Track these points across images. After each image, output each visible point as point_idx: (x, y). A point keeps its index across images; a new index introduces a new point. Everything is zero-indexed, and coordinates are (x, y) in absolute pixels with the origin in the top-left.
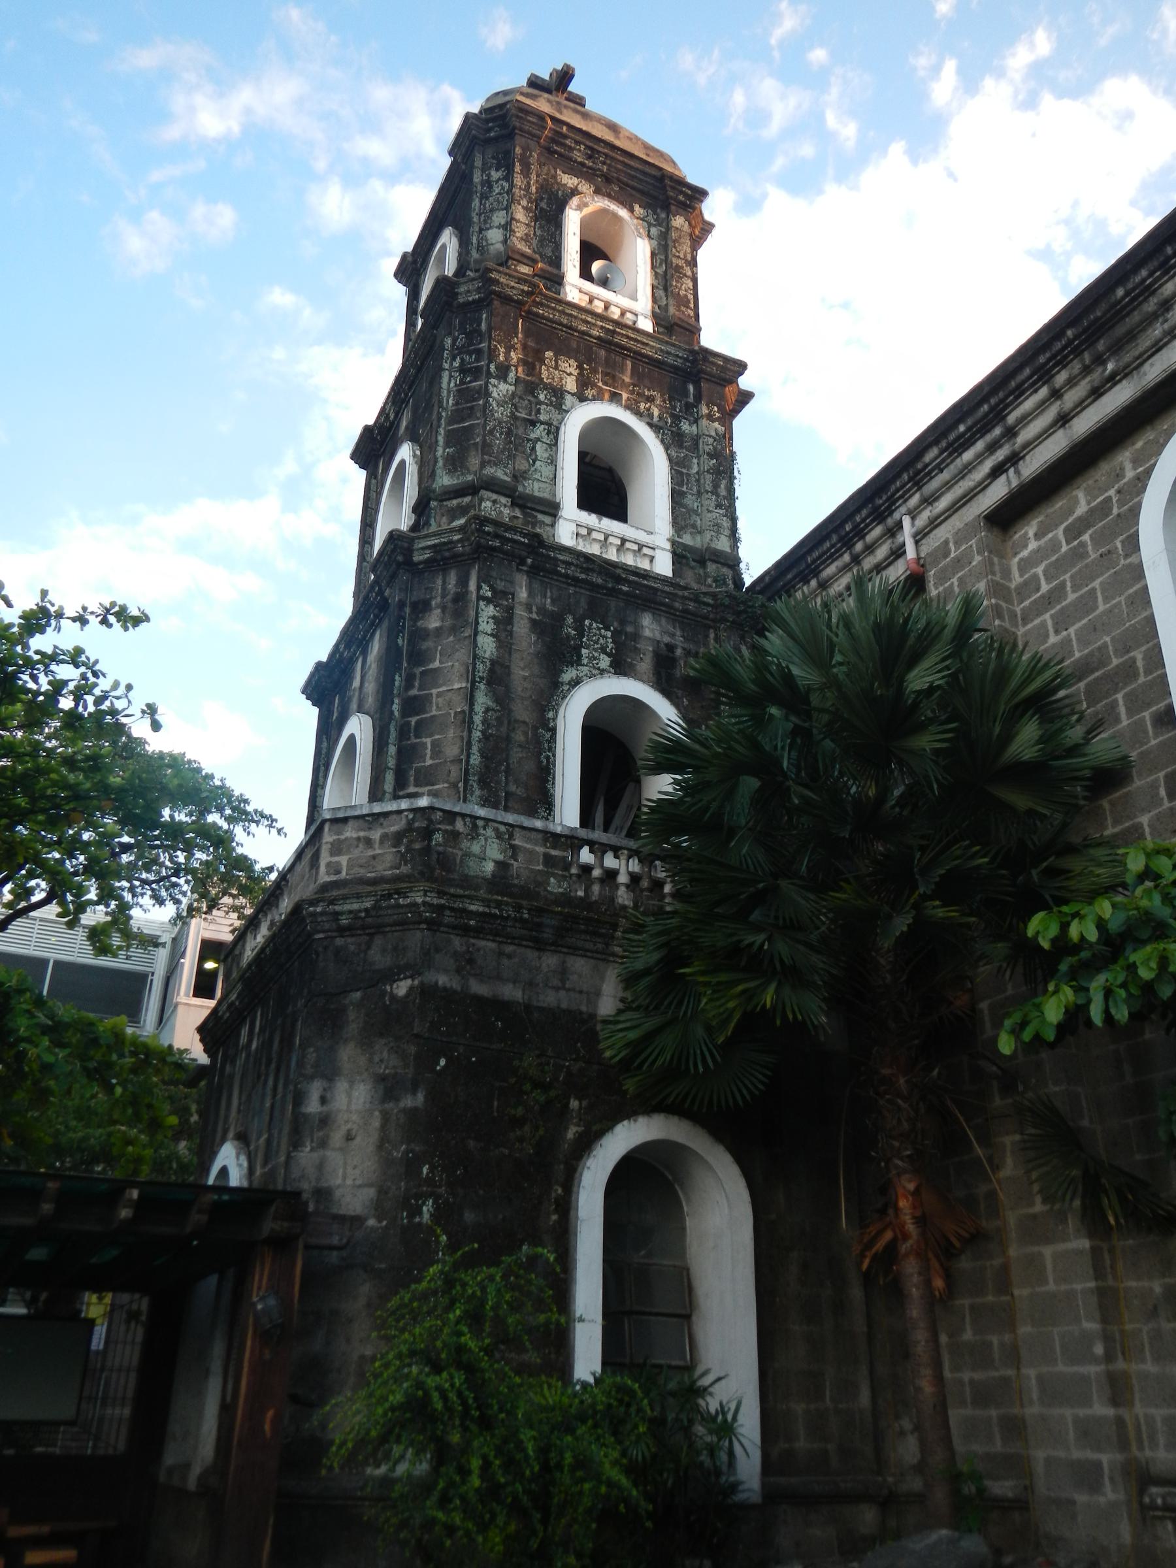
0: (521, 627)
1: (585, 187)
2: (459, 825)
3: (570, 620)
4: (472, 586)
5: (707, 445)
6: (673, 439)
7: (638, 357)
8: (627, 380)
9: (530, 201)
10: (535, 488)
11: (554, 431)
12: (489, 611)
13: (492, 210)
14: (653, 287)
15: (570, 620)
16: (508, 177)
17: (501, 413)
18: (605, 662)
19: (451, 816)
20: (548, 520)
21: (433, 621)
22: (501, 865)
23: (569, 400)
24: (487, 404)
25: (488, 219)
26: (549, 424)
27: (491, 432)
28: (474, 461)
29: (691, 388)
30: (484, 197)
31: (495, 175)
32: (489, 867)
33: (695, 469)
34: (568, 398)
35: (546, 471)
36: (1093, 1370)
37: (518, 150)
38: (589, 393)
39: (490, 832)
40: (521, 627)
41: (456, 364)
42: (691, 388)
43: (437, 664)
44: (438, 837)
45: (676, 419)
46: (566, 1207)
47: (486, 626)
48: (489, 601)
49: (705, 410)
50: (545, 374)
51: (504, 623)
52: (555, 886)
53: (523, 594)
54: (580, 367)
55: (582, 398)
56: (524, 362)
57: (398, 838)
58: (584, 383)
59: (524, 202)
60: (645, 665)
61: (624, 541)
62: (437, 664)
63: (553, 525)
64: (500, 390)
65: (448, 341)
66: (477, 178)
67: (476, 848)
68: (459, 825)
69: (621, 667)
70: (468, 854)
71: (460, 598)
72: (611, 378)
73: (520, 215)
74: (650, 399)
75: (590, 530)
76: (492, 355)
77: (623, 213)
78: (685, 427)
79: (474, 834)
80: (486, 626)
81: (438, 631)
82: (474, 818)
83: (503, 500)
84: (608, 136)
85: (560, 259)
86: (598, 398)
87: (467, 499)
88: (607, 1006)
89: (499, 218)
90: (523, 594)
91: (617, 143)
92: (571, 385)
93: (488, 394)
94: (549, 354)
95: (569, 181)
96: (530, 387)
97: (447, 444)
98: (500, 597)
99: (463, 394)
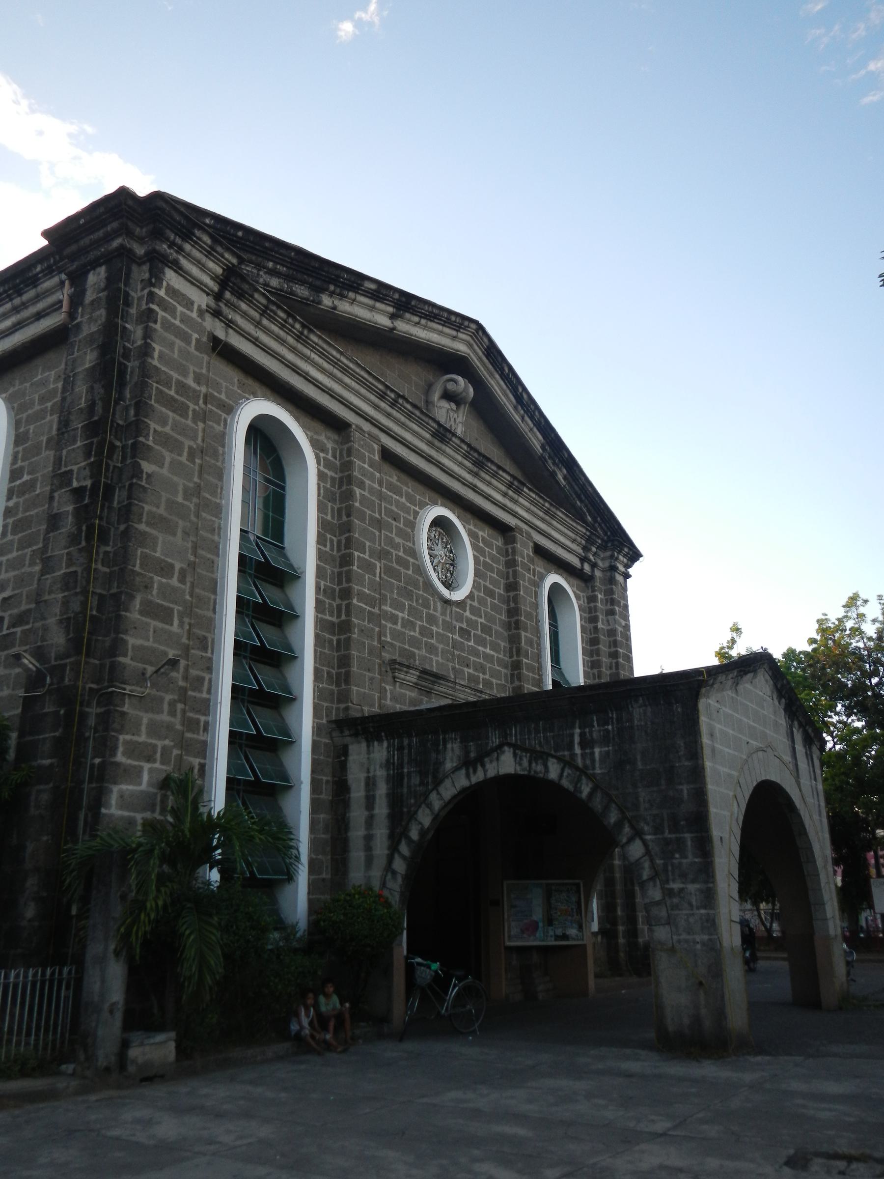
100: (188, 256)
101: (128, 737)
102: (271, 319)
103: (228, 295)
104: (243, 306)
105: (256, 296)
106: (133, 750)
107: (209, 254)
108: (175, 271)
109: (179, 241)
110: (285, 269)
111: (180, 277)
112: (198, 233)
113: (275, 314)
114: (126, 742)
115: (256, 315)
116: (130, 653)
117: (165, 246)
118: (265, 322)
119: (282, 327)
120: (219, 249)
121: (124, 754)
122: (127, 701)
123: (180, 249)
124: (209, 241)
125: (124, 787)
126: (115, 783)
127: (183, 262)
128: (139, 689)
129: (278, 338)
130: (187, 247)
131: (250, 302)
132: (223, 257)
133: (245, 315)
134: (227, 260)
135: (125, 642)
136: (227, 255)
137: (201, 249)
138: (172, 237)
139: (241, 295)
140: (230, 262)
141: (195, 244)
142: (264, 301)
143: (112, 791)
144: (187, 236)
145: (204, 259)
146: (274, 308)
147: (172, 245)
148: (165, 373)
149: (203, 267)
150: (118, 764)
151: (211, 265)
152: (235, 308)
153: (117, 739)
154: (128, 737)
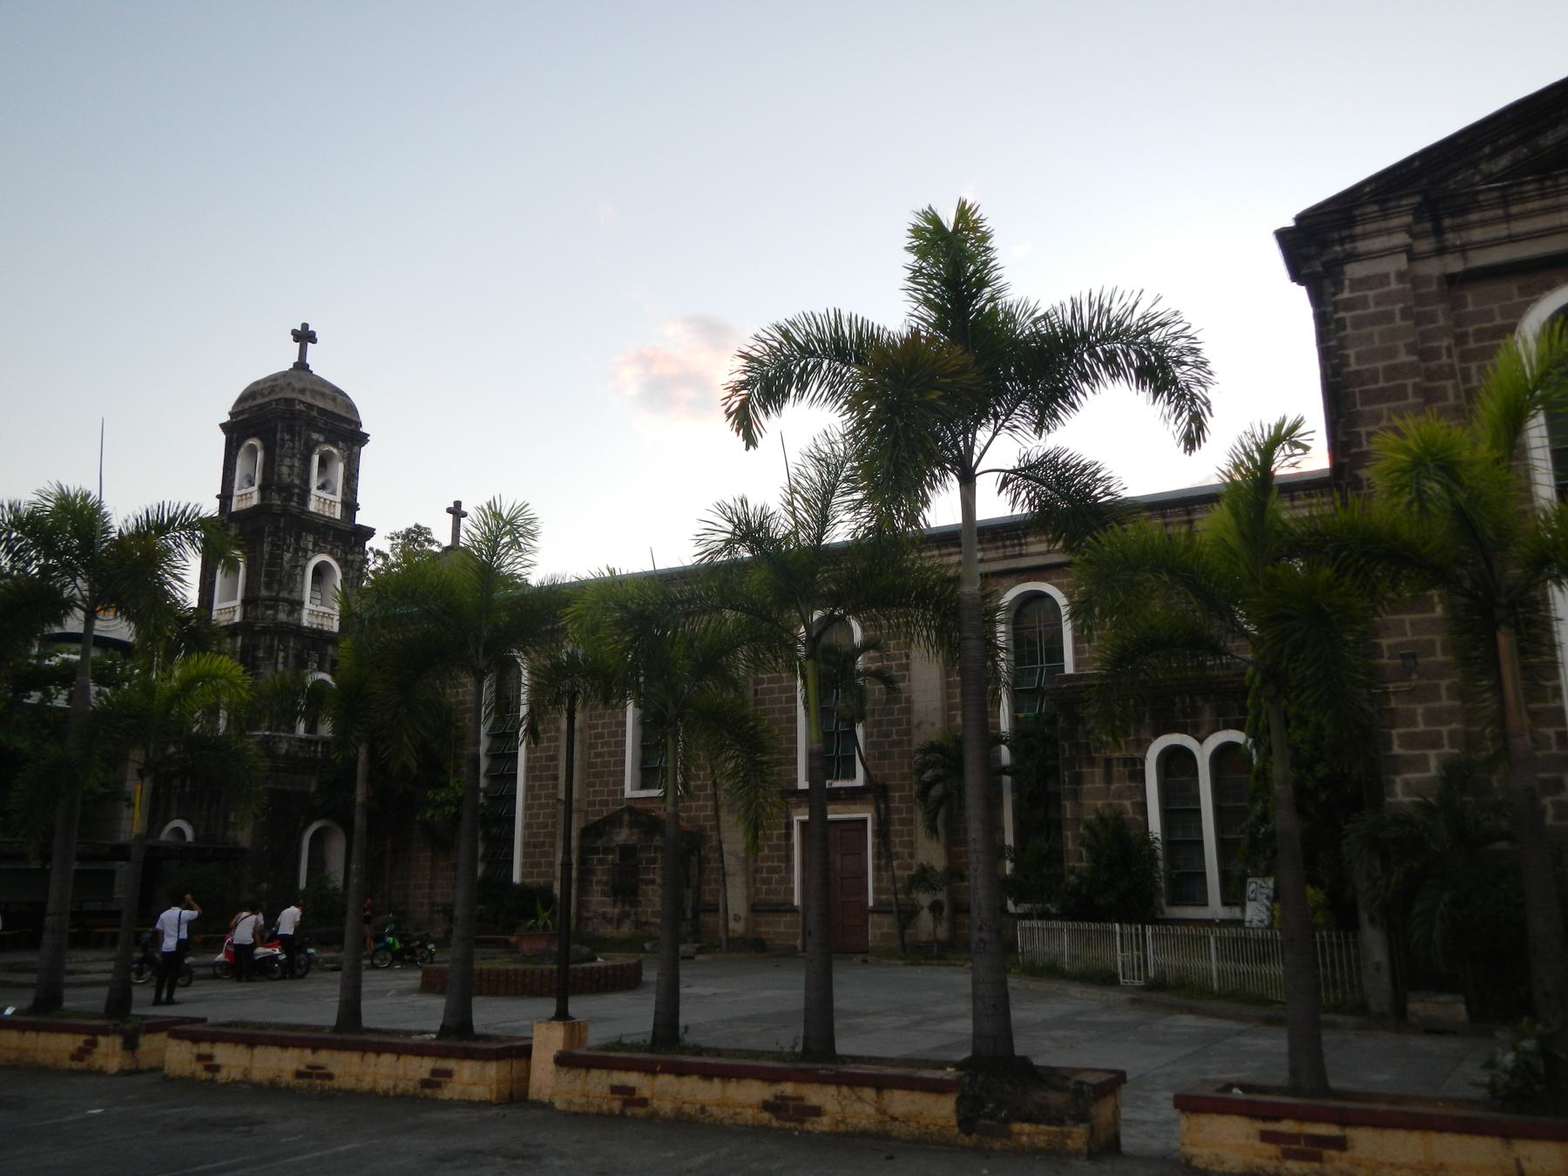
0: (291, 656)
1: (321, 439)
2: (277, 739)
3: (305, 652)
4: (276, 642)
5: (356, 565)
6: (344, 564)
7: (335, 529)
8: (330, 539)
9: (302, 454)
10: (296, 596)
11: (304, 569)
12: (282, 654)
13: (285, 456)
14: (343, 484)
15: (305, 652)
16: (292, 440)
17: (287, 566)
18: (315, 666)
19: (274, 737)
20: (299, 608)
21: (261, 654)
22: (287, 750)
23: (310, 553)
24: (282, 563)
25: (281, 460)
26: (302, 566)
27: (284, 577)
28: (276, 587)
29: (353, 539)
30: (282, 447)
31: (287, 437)
32: (284, 751)
33: (351, 576)
34: (309, 552)
35: (300, 588)
36: (427, 882)
37: (297, 428)
38: (317, 549)
39: (284, 740)
40: (291, 656)
41: (270, 539)
42: (353, 539)
43: (261, 671)
44: (271, 744)
45: (346, 555)
46: (299, 845)
47: (280, 660)
48: (282, 650)
49: (357, 550)
50: (302, 544)
51: (286, 658)
52: (301, 755)
53: (292, 644)
54: (314, 538)
55: (313, 551)
56: (295, 540)
57: (259, 743)
58: (315, 544)
59: (298, 456)
60: (327, 665)
61: (324, 613)
62: (261, 671)
63: (300, 610)
64: (287, 556)
65: (267, 528)
66: (279, 436)
67: (281, 746)
68: (277, 739)
69: (320, 669)
70: (278, 748)
71: (271, 646)
72: (325, 541)
73: (297, 464)
74: (338, 547)
75: (313, 611)
76: (285, 540)
77: (335, 451)
78: (350, 557)
79: (280, 741)
80: (280, 660)
81: (262, 658)
82: (280, 737)
83: (286, 604)
84: (329, 406)
85: (309, 478)
86: (321, 552)
87: (272, 603)
88: (312, 789)
89: (287, 461)
90: (292, 644)
91: (336, 411)
92: (311, 547)
93: (282, 559)
94: (304, 534)
95: (315, 436)
96: (296, 551)
97: (265, 576)
98: (286, 648)
99: (271, 554)
100: (1365, 236)
101: (1402, 730)
102: (1523, 200)
103: (1447, 222)
104: (1474, 217)
105: (1481, 198)
106: (1410, 741)
107: (1386, 216)
108: (1356, 261)
109: (1345, 233)
110: (1513, 136)
111: (1364, 262)
112: (1356, 212)
113: (1522, 193)
114: (1400, 736)
115: (1500, 212)
116: (1386, 654)
117: (1338, 248)
118: (1515, 209)
119: (1544, 196)
120: (1392, 204)
121: (1400, 746)
122: (1392, 697)
123: (1353, 238)
124: (1375, 208)
125: (1408, 776)
126: (1397, 773)
127: (1362, 246)
128: (1405, 684)
129: (1547, 211)
130: (1358, 230)
131: (1480, 207)
132: (1401, 206)
133: (1483, 223)
134: (1407, 205)
135: (1378, 646)
136: (1404, 202)
137: (1375, 219)
138: (1336, 235)
139: (1464, 211)
140: (1412, 204)
141: (1365, 221)
142: (1495, 194)
143: (1394, 781)
144: (1351, 222)
145: (1383, 225)
146: (1515, 189)
147: (1342, 241)
148: (1367, 370)
149: (1389, 232)
150: (1397, 757)
151: (1395, 222)
152: (1468, 226)
153: (1390, 735)
154: (1402, 730)
